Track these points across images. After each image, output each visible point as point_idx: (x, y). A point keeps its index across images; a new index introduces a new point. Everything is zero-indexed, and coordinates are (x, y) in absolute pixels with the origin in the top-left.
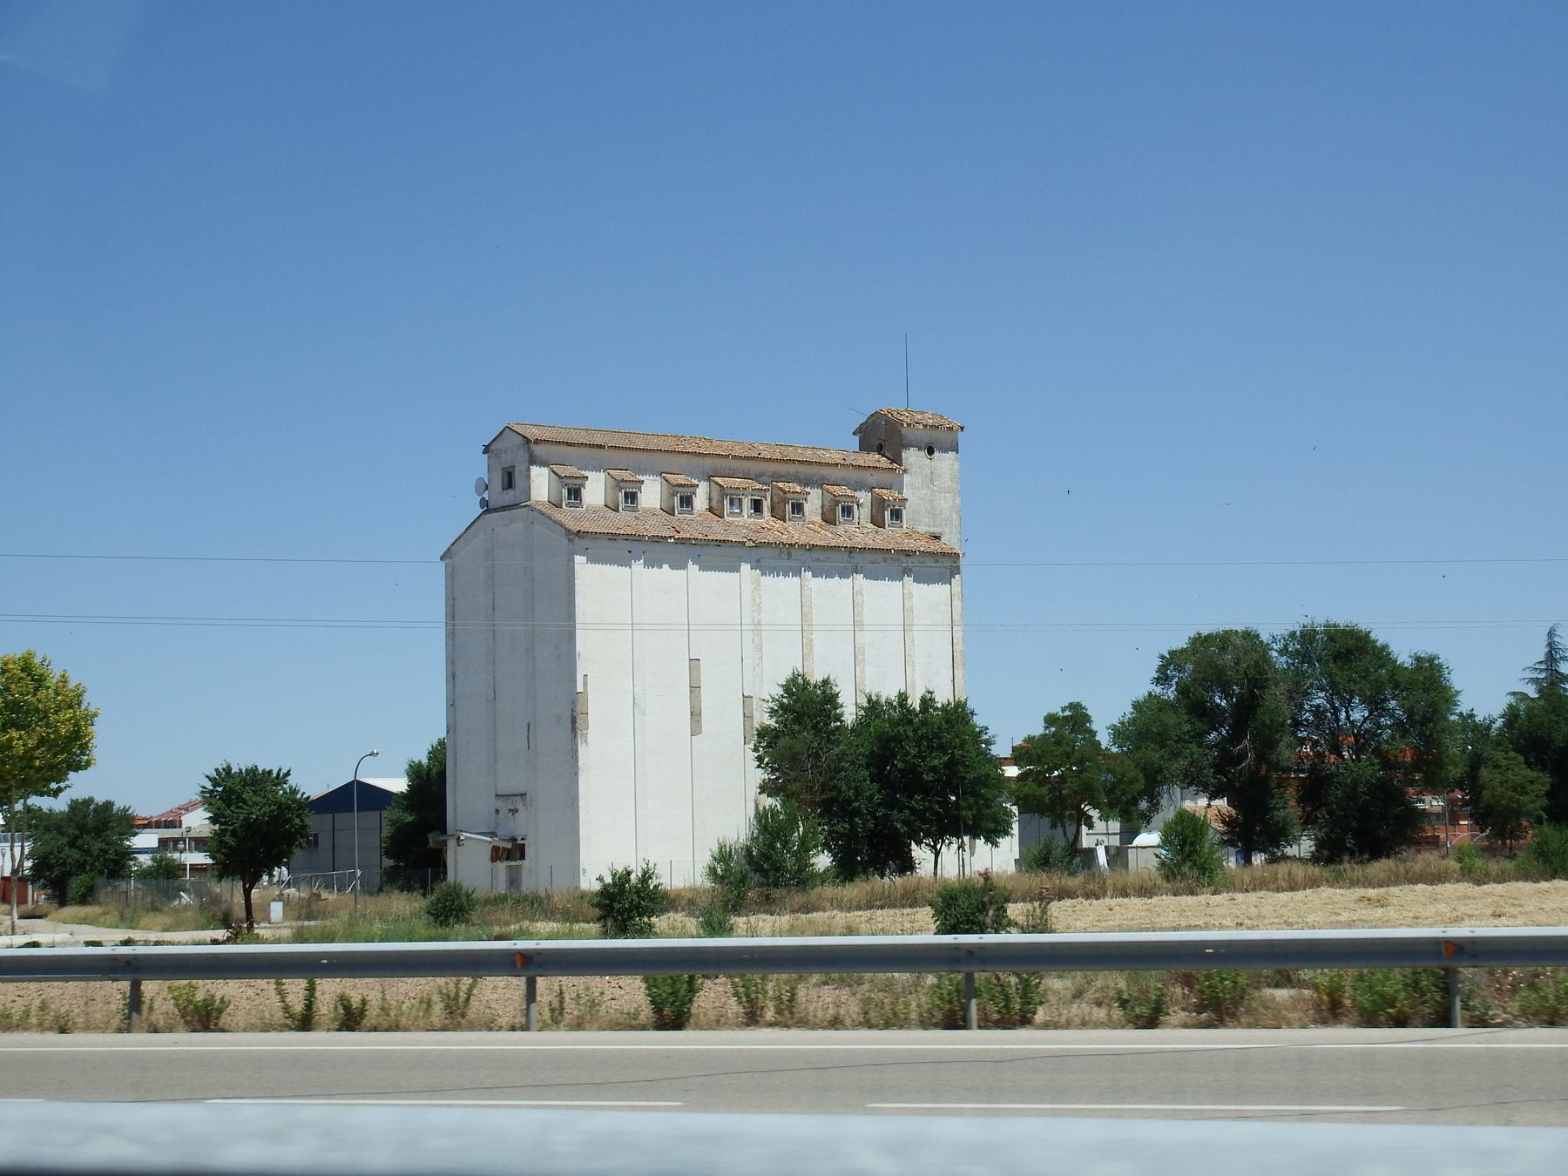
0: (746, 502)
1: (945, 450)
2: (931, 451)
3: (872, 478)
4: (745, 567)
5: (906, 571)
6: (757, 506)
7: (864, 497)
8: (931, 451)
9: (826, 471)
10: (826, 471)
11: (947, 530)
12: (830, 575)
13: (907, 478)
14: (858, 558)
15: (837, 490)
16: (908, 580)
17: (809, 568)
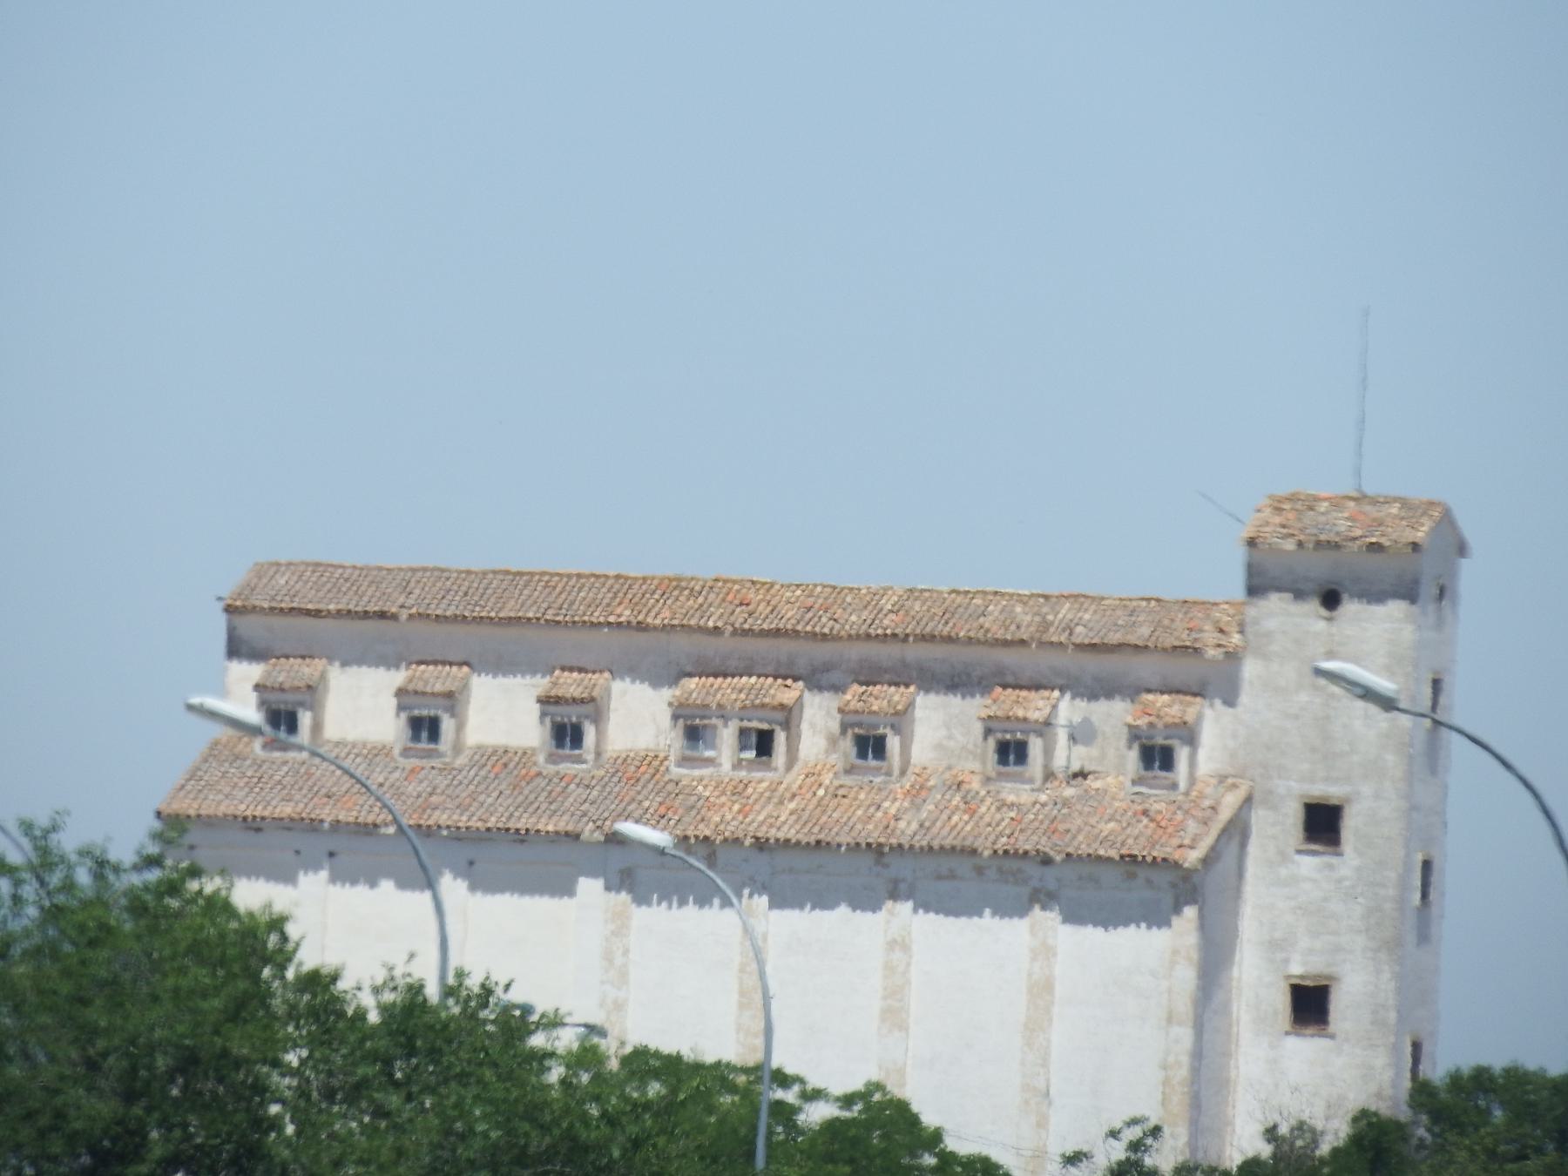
0: (727, 735)
1: (1376, 596)
2: (1331, 600)
3: (1145, 668)
4: (590, 888)
5: (1043, 897)
6: (764, 744)
7: (1114, 715)
8: (1331, 600)
9: (1008, 657)
10: (1008, 657)
11: (1366, 789)
12: (823, 902)
13: (1250, 669)
14: (901, 868)
15: (1005, 702)
16: (1046, 920)
17: (762, 888)
